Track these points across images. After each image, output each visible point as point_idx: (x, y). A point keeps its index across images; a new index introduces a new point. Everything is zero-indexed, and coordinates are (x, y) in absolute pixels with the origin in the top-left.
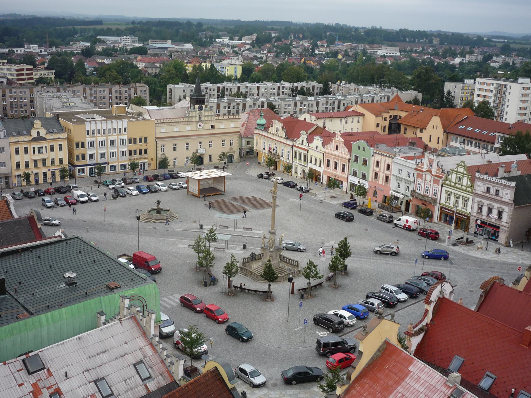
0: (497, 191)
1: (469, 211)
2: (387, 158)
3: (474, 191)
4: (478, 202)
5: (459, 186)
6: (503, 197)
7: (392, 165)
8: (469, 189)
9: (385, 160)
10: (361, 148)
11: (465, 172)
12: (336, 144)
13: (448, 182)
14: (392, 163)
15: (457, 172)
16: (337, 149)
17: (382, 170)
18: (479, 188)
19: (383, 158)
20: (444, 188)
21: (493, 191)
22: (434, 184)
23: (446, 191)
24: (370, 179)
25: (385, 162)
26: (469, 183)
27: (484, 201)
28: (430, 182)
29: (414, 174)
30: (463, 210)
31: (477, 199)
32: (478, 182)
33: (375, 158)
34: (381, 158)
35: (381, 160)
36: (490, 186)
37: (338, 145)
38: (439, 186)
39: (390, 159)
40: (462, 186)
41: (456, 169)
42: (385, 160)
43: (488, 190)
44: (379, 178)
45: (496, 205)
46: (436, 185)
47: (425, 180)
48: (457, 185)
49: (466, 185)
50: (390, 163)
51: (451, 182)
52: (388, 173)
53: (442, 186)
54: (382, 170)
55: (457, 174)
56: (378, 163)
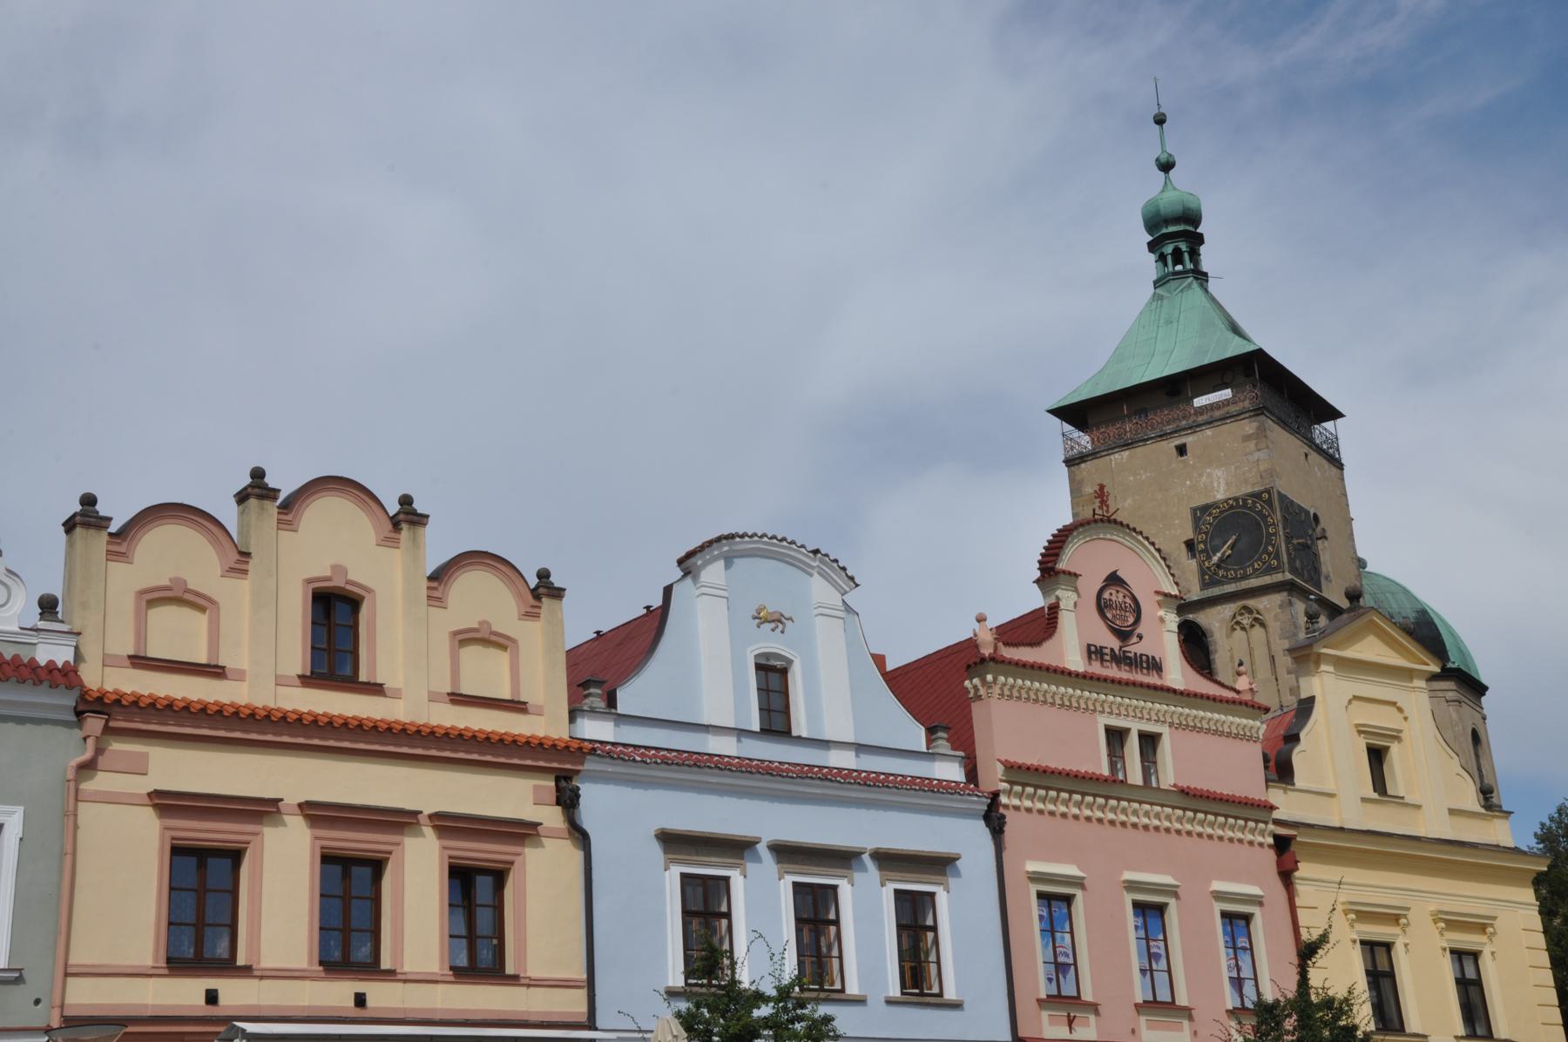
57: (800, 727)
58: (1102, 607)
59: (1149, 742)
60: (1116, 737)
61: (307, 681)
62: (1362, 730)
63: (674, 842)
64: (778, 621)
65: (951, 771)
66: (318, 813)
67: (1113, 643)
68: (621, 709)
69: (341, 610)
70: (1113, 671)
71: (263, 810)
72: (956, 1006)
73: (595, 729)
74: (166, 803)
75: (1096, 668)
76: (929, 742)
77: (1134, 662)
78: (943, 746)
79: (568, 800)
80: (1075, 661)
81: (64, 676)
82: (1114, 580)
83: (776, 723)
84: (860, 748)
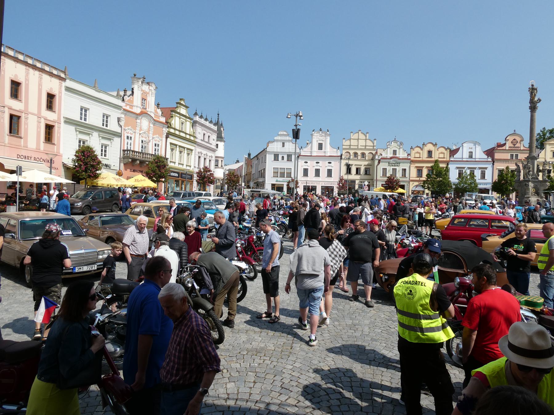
0: (209, 137)
2: (46, 77)
7: (60, 97)
8: (192, 138)
11: (187, 115)
13: (172, 131)
14: (60, 92)
17: (33, 107)
19: (34, 75)
20: (170, 140)
22: (153, 135)
23: (171, 144)
25: (40, 85)
28: (149, 130)
29: (119, 120)
31: (199, 149)
32: (198, 128)
34: (27, 74)
35: (27, 80)
38: (162, 137)
39: (56, 81)
47: (141, 130)
50: (55, 92)
51: (175, 129)
52: (51, 116)
53: (167, 137)
54: (33, 107)
55: (180, 118)
57: (473, 157)
58: (512, 142)
59: (517, 156)
60: (512, 156)
61: (427, 158)
62: (551, 151)
63: (458, 168)
64: (472, 148)
65: (490, 160)
66: (427, 167)
67: (513, 146)
68: (454, 157)
69: (430, 152)
70: (512, 149)
71: (423, 167)
72: (486, 179)
73: (451, 159)
74: (416, 167)
75: (510, 149)
76: (488, 157)
77: (516, 147)
78: (489, 158)
79: (448, 165)
80: (507, 148)
81: (410, 159)
82: (514, 139)
83: (471, 156)
84: (479, 159)
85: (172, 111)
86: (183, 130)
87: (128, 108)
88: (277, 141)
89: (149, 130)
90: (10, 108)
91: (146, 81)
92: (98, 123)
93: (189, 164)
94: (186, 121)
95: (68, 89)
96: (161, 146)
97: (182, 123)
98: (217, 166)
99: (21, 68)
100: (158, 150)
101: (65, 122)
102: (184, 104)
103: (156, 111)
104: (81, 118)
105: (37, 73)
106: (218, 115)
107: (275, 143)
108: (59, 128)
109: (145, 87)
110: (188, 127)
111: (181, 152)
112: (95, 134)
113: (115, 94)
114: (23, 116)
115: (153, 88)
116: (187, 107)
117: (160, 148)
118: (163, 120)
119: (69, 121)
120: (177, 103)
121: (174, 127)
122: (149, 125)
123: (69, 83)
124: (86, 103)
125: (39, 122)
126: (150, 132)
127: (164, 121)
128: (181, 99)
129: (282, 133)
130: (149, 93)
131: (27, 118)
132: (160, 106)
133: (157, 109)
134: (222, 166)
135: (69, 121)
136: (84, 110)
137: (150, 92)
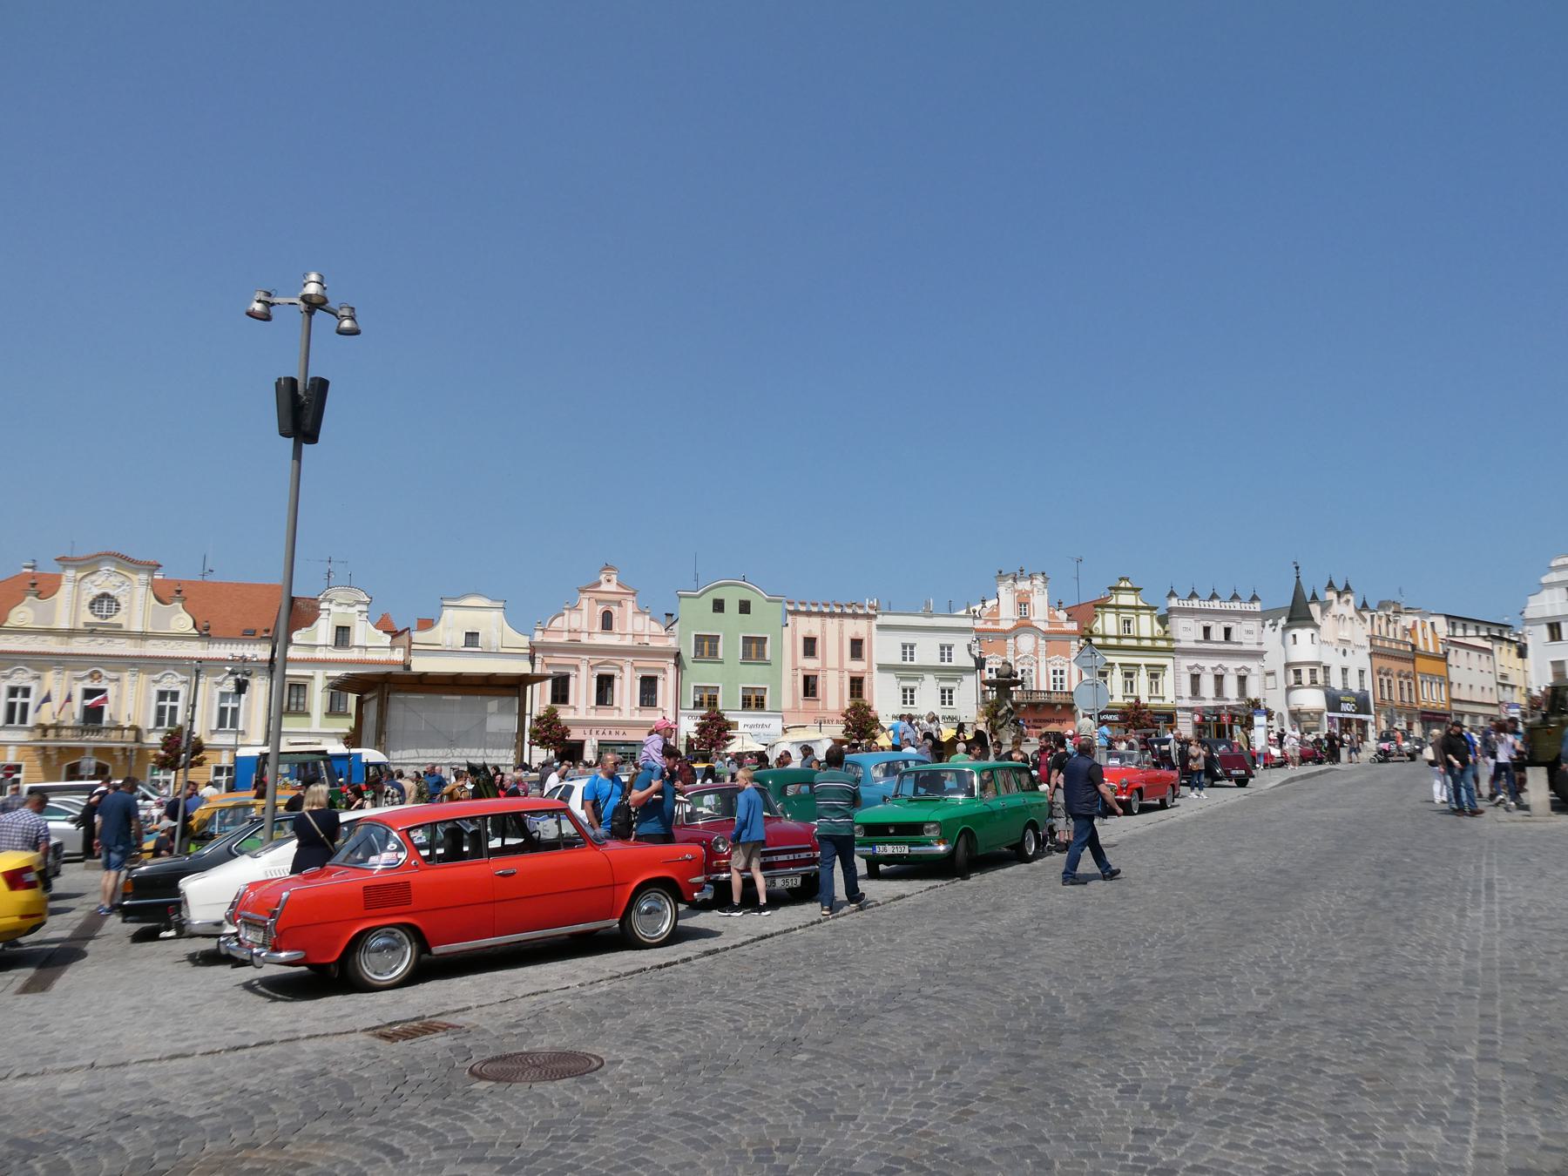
0: (1228, 631)
1: (1169, 700)
2: (848, 622)
3: (1174, 645)
4: (1190, 668)
5: (1134, 643)
6: (1242, 640)
8: (1163, 644)
9: (841, 626)
10: (732, 607)
11: (1140, 604)
12: (600, 609)
14: (870, 634)
15: (1117, 607)
16: (607, 622)
18: (1185, 633)
21: (1217, 633)
24: (787, 703)
25: (841, 632)
26: (1157, 627)
27: (1202, 662)
28: (1036, 652)
30: (1154, 702)
31: (1186, 662)
32: (1180, 620)
33: (794, 630)
34: (823, 626)
35: (824, 632)
36: (1210, 624)
37: (615, 609)
40: (1139, 639)
41: (1113, 602)
42: (841, 626)
43: (1207, 630)
44: (825, 690)
45: (1232, 665)
46: (1059, 662)
48: (1125, 642)
49: (1149, 635)
50: (863, 634)
51: (1104, 637)
52: (857, 667)
54: (832, 661)
55: (1118, 615)
56: (810, 646)
85: (1096, 606)
86: (1132, 634)
87: (990, 626)
88: (1551, 585)
89: (1036, 652)
90: (804, 669)
91: (1026, 574)
92: (936, 661)
93: (1160, 694)
94: (1138, 616)
95: (880, 627)
96: (1070, 672)
97: (1129, 622)
98: (1300, 683)
99: (816, 621)
100: (1061, 680)
101: (878, 669)
102: (1128, 585)
103: (1052, 616)
104: (905, 659)
105: (836, 621)
106: (1297, 568)
107: (1546, 593)
108: (871, 679)
109: (1024, 585)
110: (1146, 626)
111: (1128, 675)
112: (929, 678)
113: (963, 612)
114: (820, 674)
115: (1039, 581)
116: (1136, 590)
117: (1065, 676)
118: (1073, 626)
119: (883, 668)
120: (1110, 588)
121: (1101, 633)
122: (1036, 643)
123: (881, 620)
124: (909, 638)
125: (841, 678)
126: (1040, 653)
127: (1076, 629)
128: (1121, 579)
129: (1560, 562)
130: (1032, 591)
131: (824, 677)
132: (1064, 606)
133: (1057, 613)
134: (1314, 682)
135: (883, 668)
136: (908, 649)
137: (1035, 589)
